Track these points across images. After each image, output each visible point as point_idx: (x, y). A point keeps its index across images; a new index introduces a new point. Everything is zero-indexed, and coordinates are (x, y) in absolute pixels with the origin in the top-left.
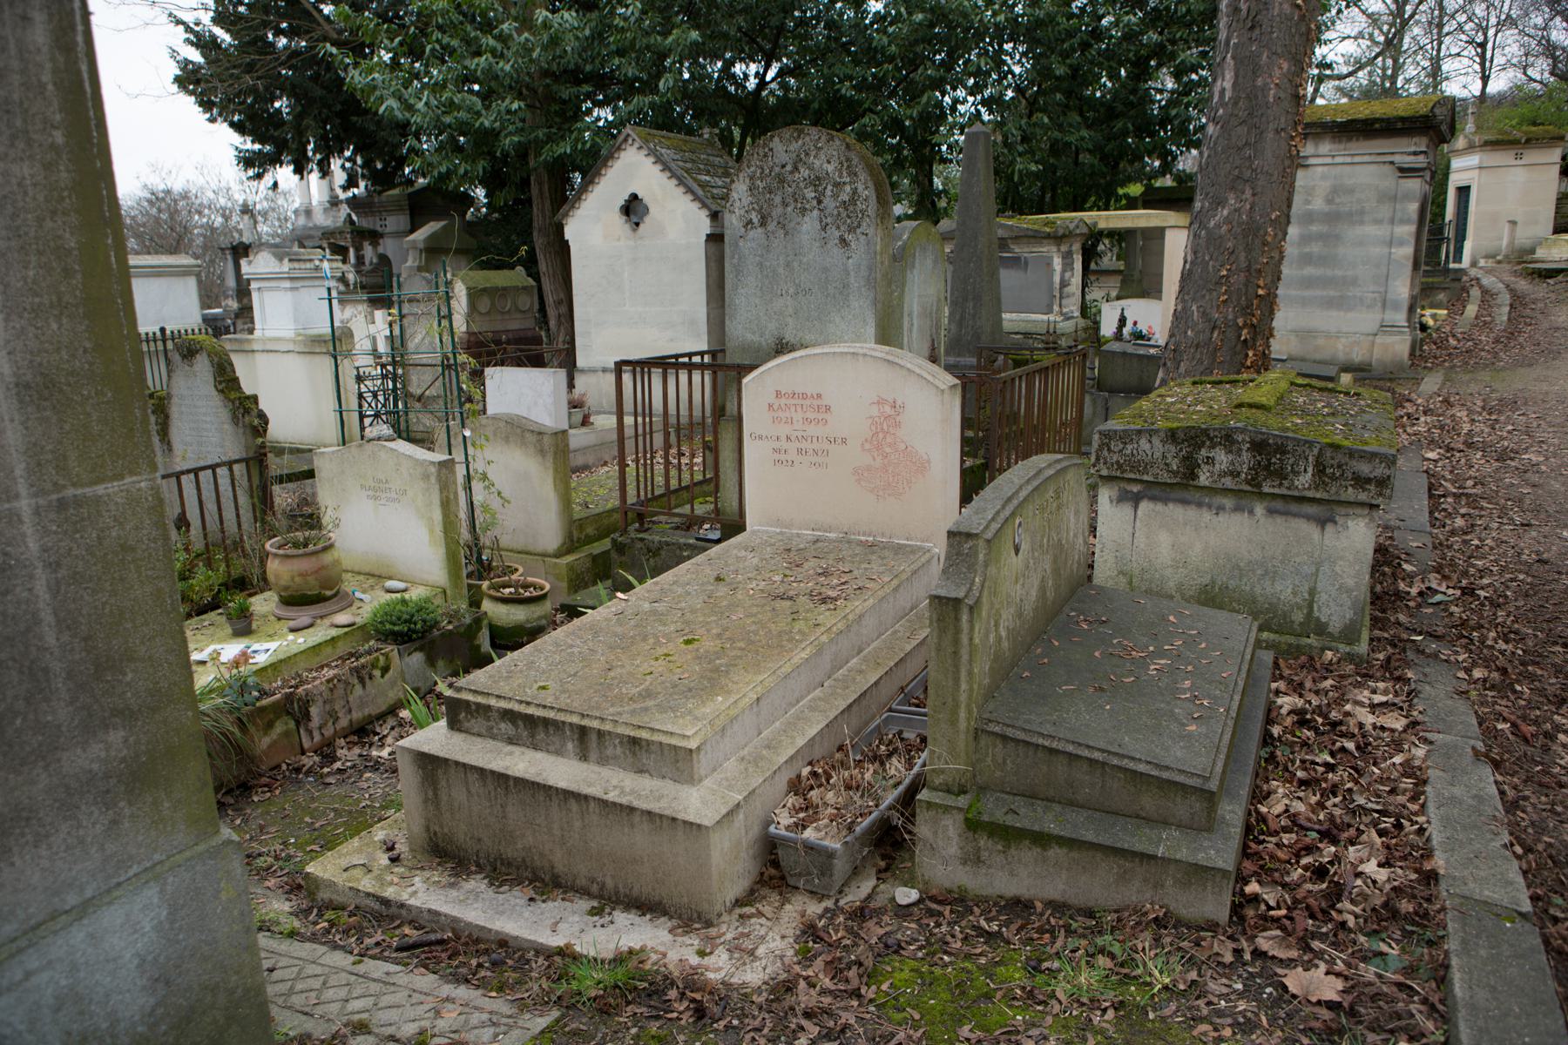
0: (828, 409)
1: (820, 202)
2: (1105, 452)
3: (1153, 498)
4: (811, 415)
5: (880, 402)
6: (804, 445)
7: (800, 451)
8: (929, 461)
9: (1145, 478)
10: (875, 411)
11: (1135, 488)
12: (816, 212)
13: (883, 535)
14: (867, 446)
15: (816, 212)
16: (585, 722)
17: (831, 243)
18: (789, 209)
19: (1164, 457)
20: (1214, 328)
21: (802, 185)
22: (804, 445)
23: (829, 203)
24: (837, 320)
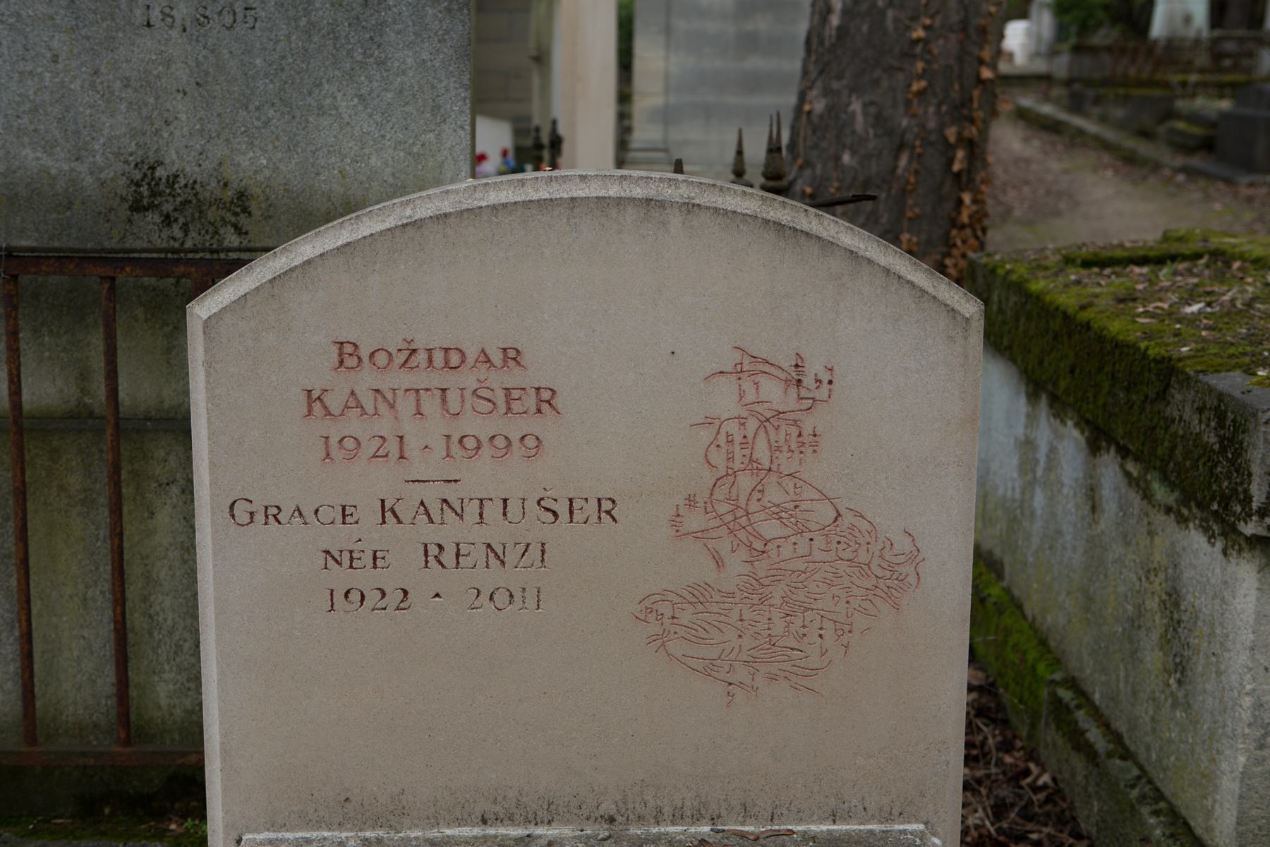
5: (749, 366)
6: (450, 532)
7: (432, 554)
8: (915, 557)
10: (725, 401)
13: (747, 813)
14: (694, 521)
22: (450, 532)
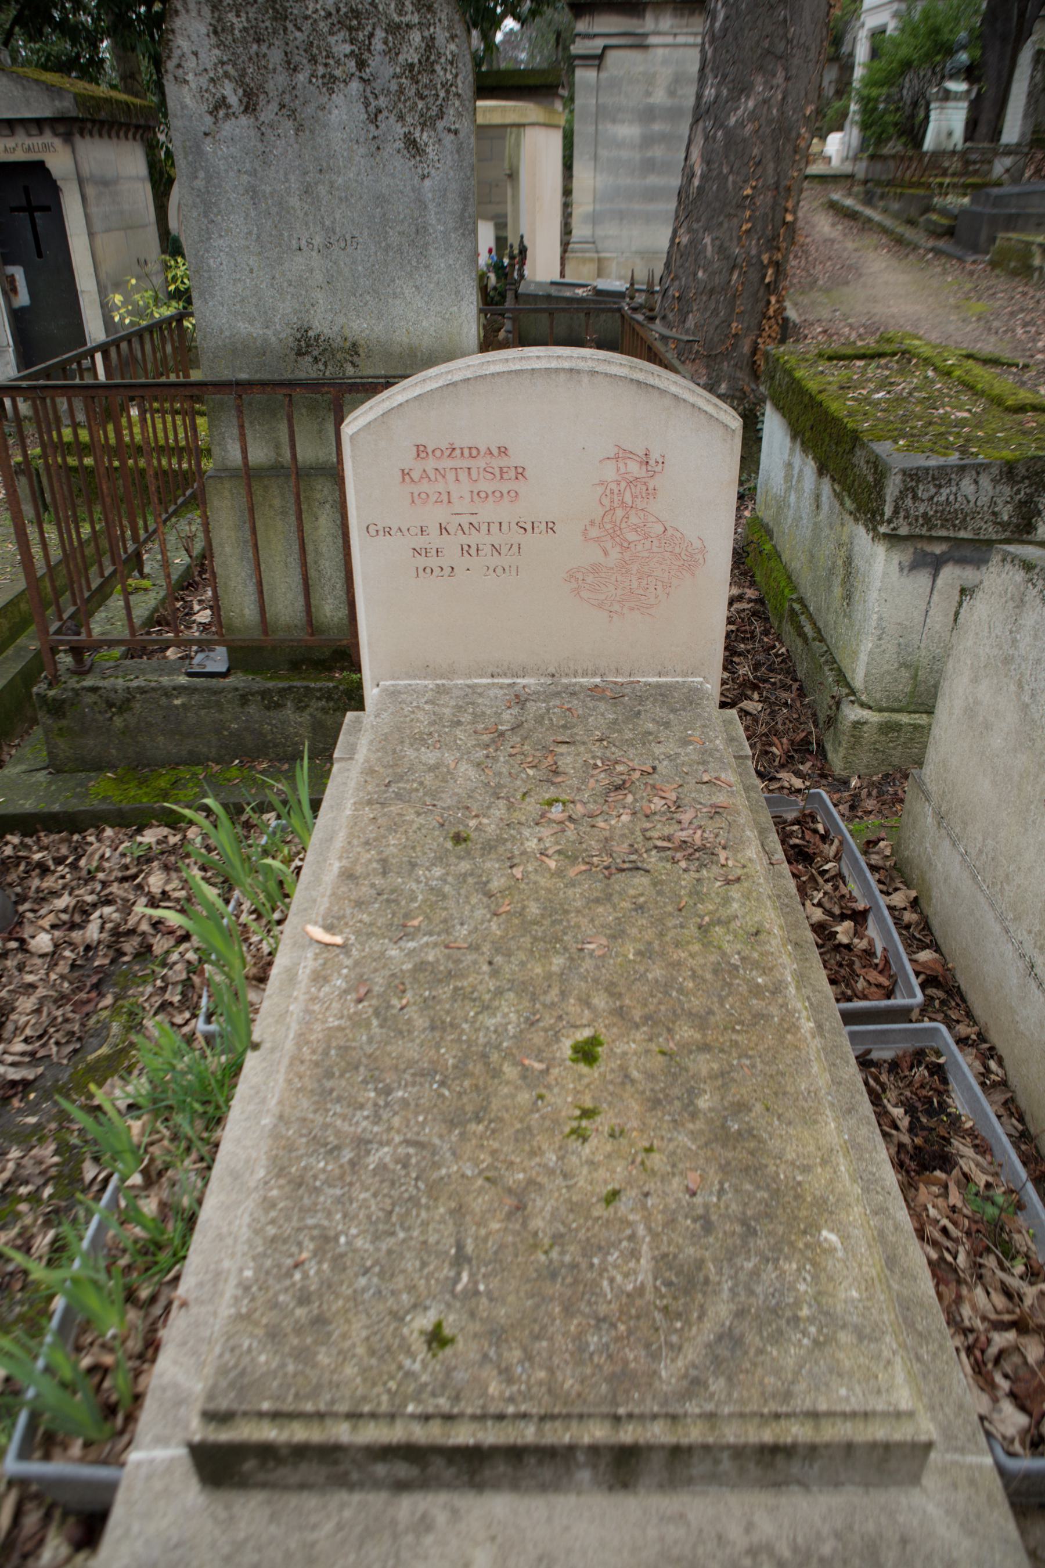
0: (520, 473)
1: (361, 64)
2: (909, 501)
3: (962, 561)
4: (485, 486)
5: (622, 455)
6: (473, 539)
7: (465, 550)
8: (703, 550)
9: (962, 534)
10: (610, 473)
11: (938, 549)
12: (355, 85)
13: (618, 672)
14: (594, 532)
15: (355, 85)
16: (628, 1435)
17: (389, 149)
18: (301, 77)
19: (993, 503)
20: (734, 267)
21: (323, 26)
22: (473, 539)
23: (376, 63)
24: (408, 292)
